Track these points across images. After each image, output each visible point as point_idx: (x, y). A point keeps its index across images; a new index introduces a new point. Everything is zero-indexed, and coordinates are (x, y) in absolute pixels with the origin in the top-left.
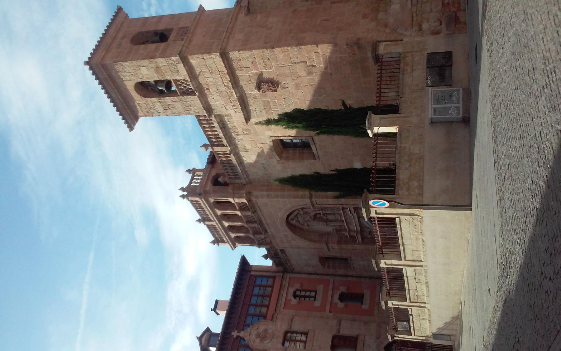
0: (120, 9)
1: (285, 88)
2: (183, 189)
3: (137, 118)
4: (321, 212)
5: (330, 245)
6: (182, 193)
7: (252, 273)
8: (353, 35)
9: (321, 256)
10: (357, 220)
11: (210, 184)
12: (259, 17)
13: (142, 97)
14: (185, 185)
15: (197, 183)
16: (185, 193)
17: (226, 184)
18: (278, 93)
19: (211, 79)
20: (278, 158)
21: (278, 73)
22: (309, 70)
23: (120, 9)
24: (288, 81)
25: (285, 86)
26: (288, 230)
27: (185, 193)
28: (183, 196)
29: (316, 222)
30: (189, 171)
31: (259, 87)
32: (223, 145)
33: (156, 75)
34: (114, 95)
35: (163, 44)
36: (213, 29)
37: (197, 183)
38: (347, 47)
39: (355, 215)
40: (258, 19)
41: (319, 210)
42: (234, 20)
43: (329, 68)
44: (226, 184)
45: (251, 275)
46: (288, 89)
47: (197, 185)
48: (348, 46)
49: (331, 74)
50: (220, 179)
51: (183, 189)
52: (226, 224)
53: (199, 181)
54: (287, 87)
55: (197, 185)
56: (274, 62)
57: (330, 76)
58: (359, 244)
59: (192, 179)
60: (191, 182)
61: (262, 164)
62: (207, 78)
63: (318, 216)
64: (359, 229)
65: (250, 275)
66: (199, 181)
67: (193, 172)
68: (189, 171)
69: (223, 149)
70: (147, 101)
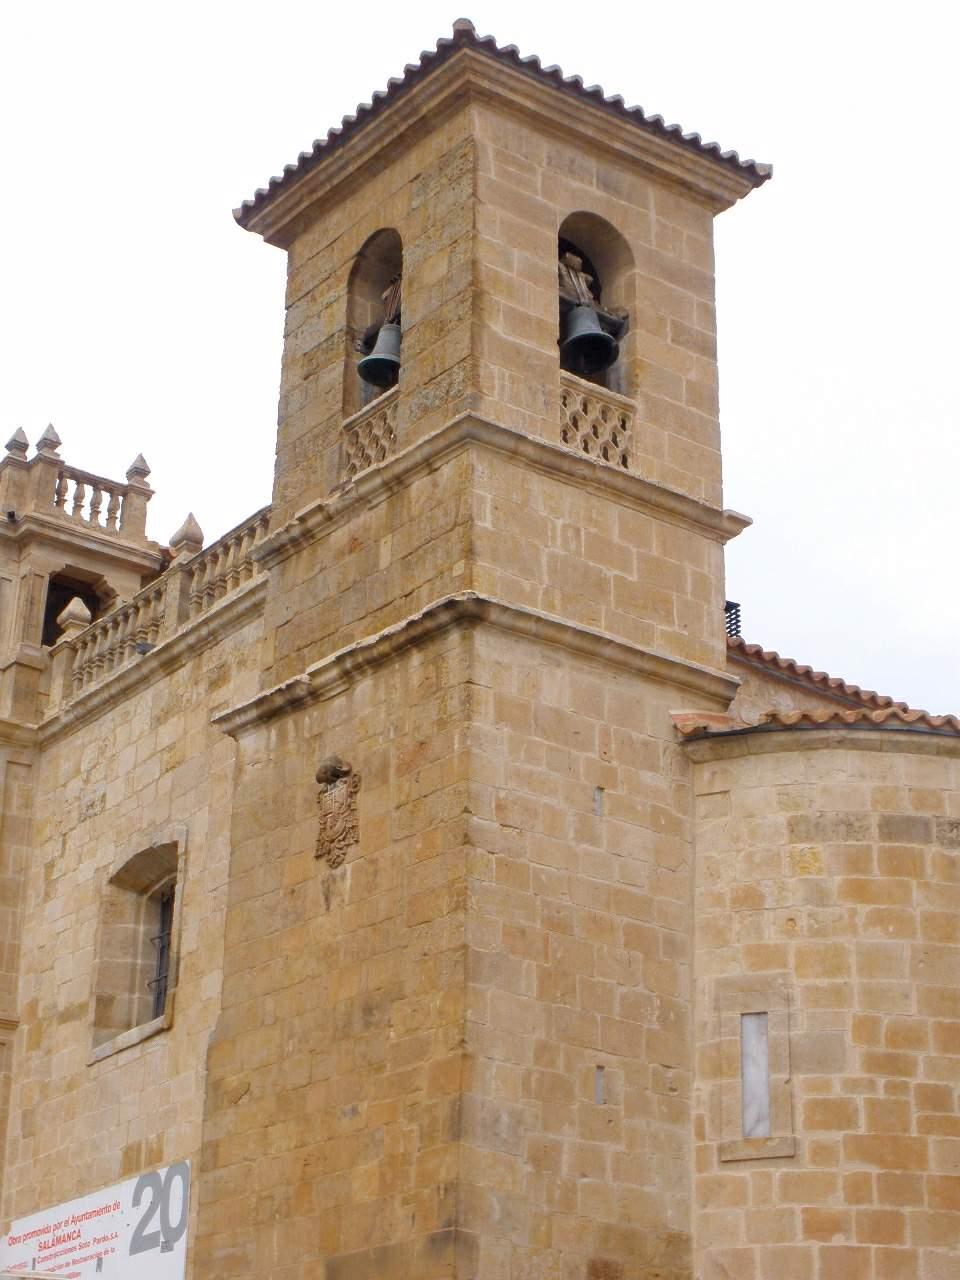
0: (754, 175)
1: (327, 899)
2: (50, 442)
3: (281, 237)
6: (33, 439)
8: (497, 1216)
11: (60, 561)
12: (659, 780)
13: (352, 262)
14: (69, 455)
15: (78, 507)
16: (31, 454)
17: (51, 631)
18: (312, 863)
19: (384, 562)
23: (754, 175)
24: (347, 908)
27: (31, 454)
28: (18, 445)
30: (139, 471)
32: (183, 617)
33: (418, 318)
34: (358, 142)
35: (555, 353)
36: (609, 574)
37: (78, 507)
38: (442, 1186)
40: (647, 777)
42: (647, 665)
44: (51, 631)
46: (323, 909)
47: (68, 507)
48: (442, 1192)
50: (77, 606)
51: (50, 442)
53: (86, 513)
54: (332, 908)
55: (68, 507)
59: (99, 484)
60: (82, 478)
62: (389, 543)
66: (86, 513)
67: (134, 490)
68: (139, 471)
69: (171, 620)
70: (339, 280)
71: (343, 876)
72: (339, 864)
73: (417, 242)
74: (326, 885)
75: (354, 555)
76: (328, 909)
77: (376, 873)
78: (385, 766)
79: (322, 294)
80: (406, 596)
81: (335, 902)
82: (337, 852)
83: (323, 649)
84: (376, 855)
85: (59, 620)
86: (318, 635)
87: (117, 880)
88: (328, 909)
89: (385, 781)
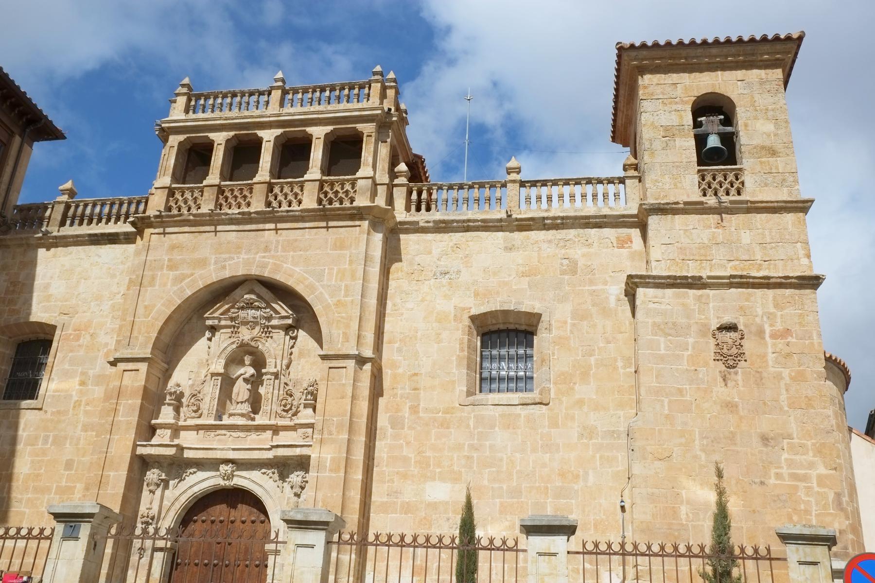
1: (724, 380)
4: (270, 368)
5: (143, 367)
7: (17, 139)
9: (58, 332)
10: (232, 455)
18: (712, 363)
20: (475, 311)
21: (765, 375)
22: (772, 439)
25: (729, 382)
26: (227, 274)
29: (229, 349)
31: (731, 328)
34: (714, 51)
39: (270, 455)
41: (276, 367)
43: (779, 482)
45: (12, 135)
49: (762, 483)
52: (268, 136)
54: (729, 385)
56: (793, 374)
57: (757, 480)
58: (135, 446)
61: (459, 272)
63: (247, 359)
64: (187, 454)
65: (13, 132)
71: (736, 373)
72: (734, 367)
73: (748, 109)
74: (723, 373)
75: (720, 231)
76: (726, 385)
77: (762, 379)
78: (761, 333)
79: (670, 103)
80: (765, 261)
81: (730, 384)
82: (734, 362)
83: (704, 265)
84: (760, 370)
85: (396, 170)
86: (697, 258)
87: (473, 318)
88: (726, 385)
89: (764, 338)
